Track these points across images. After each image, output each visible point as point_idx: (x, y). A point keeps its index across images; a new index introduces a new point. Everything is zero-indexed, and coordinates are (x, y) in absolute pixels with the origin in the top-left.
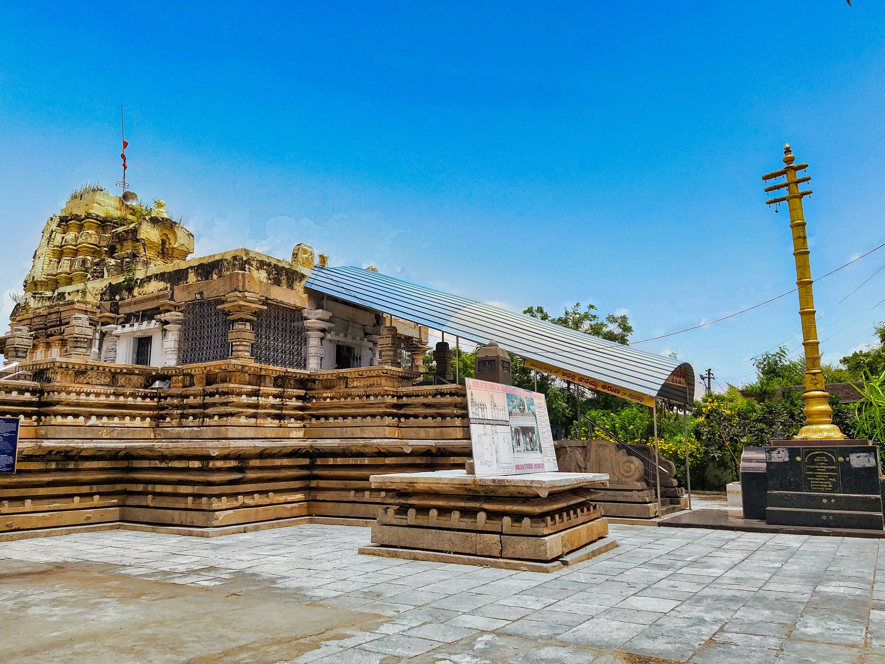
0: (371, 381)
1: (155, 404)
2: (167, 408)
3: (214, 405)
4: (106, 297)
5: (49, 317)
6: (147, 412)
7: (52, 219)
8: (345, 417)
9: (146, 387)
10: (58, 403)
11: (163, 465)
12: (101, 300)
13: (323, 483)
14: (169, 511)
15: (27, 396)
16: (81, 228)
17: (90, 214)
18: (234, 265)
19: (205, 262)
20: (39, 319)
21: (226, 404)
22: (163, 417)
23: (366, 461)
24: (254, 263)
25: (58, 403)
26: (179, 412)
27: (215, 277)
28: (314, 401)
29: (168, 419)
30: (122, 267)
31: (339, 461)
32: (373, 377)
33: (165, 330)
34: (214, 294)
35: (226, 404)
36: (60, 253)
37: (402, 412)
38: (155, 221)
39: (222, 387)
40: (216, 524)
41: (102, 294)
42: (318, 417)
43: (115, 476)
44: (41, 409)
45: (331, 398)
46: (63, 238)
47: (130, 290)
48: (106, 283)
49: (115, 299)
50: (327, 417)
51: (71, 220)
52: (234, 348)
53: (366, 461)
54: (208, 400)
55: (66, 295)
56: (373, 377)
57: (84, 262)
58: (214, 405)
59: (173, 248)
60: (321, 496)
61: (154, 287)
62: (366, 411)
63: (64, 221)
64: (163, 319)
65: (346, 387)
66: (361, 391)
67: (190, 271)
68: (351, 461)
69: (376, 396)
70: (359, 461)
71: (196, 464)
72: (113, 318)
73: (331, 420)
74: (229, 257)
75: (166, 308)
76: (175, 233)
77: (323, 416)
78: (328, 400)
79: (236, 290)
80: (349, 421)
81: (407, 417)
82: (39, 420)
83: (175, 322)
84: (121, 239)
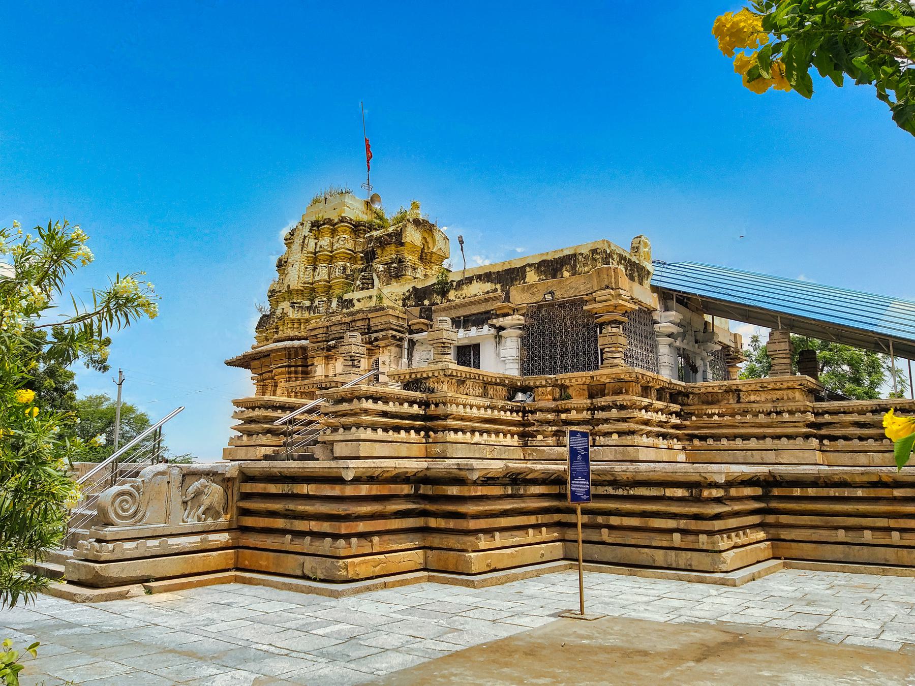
0: (778, 394)
1: (520, 419)
2: (534, 424)
3: (607, 421)
4: (411, 302)
5: (353, 324)
6: (515, 429)
7: (302, 224)
8: (746, 437)
9: (510, 399)
10: (446, 417)
11: (620, 492)
12: (404, 306)
13: (784, 519)
14: (646, 550)
15: (415, 409)
16: (333, 232)
17: (345, 218)
18: (595, 260)
19: (549, 258)
20: (339, 327)
21: (624, 420)
22: (533, 435)
23: (860, 493)
24: (615, 256)
25: (446, 417)
26: (554, 428)
28: (694, 418)
29: (540, 437)
30: (390, 273)
31: (811, 492)
32: (781, 389)
33: (500, 337)
34: (571, 293)
35: (624, 420)
36: (314, 260)
37: (823, 432)
38: (417, 223)
39: (619, 399)
40: (725, 569)
41: (404, 300)
42: (703, 438)
43: (515, 506)
44: (428, 424)
45: (719, 415)
46: (316, 244)
47: (444, 293)
48: (409, 287)
49: (422, 304)
50: (717, 438)
51: (324, 224)
52: (605, 356)
53: (860, 493)
54: (599, 415)
55: (355, 302)
56: (781, 389)
57: (344, 268)
58: (607, 421)
59: (432, 253)
60: (785, 534)
61: (477, 289)
62: (778, 431)
63: (316, 226)
64: (497, 325)
65: (738, 402)
66: (769, 407)
67: (528, 269)
68: (832, 492)
69: (791, 413)
70: (846, 492)
71: (679, 492)
72: (427, 325)
73: (724, 441)
74: (585, 251)
75: (505, 311)
76: (433, 237)
77: (711, 437)
78: (716, 417)
79: (608, 287)
80: (753, 443)
81: (833, 438)
82: (427, 436)
83: (513, 327)
84: (383, 243)
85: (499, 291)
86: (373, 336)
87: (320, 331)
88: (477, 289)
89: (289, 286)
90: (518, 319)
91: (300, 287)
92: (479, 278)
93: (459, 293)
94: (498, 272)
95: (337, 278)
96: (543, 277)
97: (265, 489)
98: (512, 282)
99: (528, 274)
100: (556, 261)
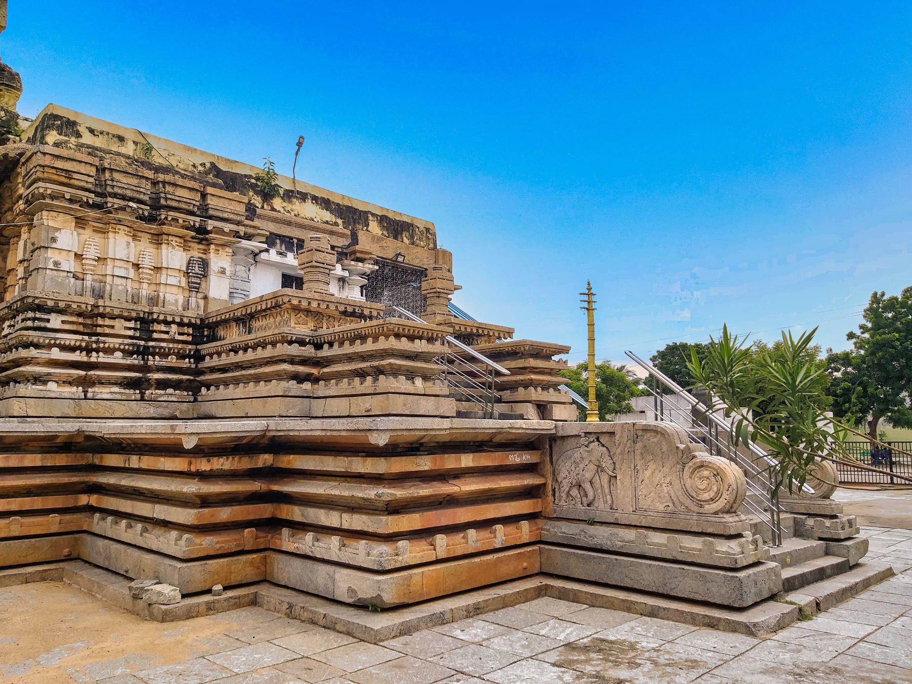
5: (169, 188)
19: (391, 216)
20: (135, 181)
27: (405, 240)
61: (310, 211)
67: (370, 218)
85: (341, 227)
86: (211, 224)
87: (83, 168)
88: (310, 211)
90: (368, 267)
92: (315, 199)
93: (289, 207)
94: (338, 205)
96: (385, 233)
98: (355, 224)
99: (371, 223)
100: (398, 222)
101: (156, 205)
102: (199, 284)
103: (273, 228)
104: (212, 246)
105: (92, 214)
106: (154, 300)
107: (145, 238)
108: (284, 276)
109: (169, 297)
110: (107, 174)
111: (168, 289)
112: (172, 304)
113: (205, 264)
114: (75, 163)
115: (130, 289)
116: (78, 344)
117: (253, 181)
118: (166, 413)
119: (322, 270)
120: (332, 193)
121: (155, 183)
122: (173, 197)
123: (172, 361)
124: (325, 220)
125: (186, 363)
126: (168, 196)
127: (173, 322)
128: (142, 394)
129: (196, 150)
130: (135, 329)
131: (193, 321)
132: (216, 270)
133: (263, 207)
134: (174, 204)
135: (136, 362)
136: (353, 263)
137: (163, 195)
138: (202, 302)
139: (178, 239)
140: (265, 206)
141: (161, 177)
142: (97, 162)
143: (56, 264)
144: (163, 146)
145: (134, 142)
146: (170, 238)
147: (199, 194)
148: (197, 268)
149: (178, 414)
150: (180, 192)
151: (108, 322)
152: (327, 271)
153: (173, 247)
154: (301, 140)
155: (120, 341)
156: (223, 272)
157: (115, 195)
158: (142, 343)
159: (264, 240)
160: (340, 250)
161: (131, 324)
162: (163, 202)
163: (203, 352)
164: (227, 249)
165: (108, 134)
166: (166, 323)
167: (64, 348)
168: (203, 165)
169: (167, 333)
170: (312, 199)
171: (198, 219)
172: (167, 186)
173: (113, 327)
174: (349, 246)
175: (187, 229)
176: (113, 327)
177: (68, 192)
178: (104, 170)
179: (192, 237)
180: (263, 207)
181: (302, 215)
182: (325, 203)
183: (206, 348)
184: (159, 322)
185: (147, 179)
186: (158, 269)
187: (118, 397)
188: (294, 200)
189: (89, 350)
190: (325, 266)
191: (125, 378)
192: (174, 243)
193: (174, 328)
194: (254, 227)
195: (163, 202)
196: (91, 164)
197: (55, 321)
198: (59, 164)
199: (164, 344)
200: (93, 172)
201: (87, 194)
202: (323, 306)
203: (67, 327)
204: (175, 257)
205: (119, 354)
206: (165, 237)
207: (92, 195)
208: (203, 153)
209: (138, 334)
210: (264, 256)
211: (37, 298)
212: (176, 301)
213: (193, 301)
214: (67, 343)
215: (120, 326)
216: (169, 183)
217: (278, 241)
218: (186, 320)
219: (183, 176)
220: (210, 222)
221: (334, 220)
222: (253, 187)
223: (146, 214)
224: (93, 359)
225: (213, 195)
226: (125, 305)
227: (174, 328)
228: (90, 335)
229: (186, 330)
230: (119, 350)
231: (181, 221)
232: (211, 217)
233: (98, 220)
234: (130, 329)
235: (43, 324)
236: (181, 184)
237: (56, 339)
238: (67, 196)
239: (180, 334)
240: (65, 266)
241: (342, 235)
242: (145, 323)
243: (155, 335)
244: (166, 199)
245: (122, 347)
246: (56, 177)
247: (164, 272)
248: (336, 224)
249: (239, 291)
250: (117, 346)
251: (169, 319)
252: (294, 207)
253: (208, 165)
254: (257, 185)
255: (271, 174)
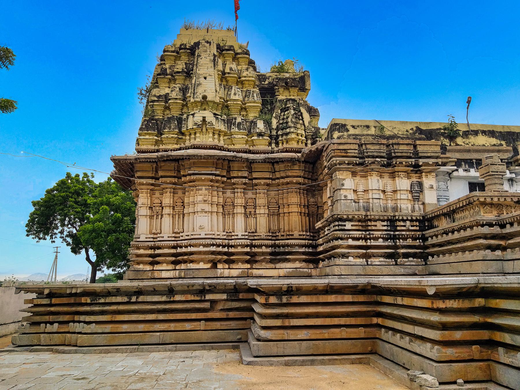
5: (395, 147)
20: (377, 147)
85: (505, 146)
86: (421, 161)
87: (352, 146)
88: (482, 140)
89: (204, 97)
91: (217, 100)
92: (484, 132)
93: (467, 141)
94: (500, 132)
95: (254, 102)
97: (433, 303)
101: (390, 157)
102: (419, 196)
103: (458, 156)
104: (424, 174)
105: (359, 168)
106: (395, 209)
107: (386, 176)
108: (470, 184)
109: (403, 206)
110: (364, 147)
111: (402, 201)
112: (405, 210)
113: (420, 185)
114: (348, 145)
115: (382, 204)
116: (360, 236)
117: (442, 131)
118: (410, 271)
119: (497, 176)
120: (495, 126)
121: (388, 146)
122: (398, 151)
123: (410, 242)
124: (492, 144)
125: (417, 243)
126: (396, 151)
127: (407, 220)
128: (396, 261)
129: (407, 122)
130: (387, 226)
131: (418, 218)
132: (428, 187)
133: (450, 145)
134: (399, 154)
135: (390, 244)
136: (517, 167)
137: (393, 151)
138: (421, 207)
139: (403, 173)
140: (452, 144)
141: (391, 141)
142: (358, 142)
143: (345, 196)
144: (389, 125)
145: (374, 127)
146: (400, 173)
147: (412, 146)
148: (416, 188)
149: (417, 272)
150: (402, 147)
151: (373, 223)
152: (501, 176)
153: (402, 178)
154: (470, 99)
155: (380, 233)
156: (432, 187)
157: (368, 157)
158: (392, 233)
159: (454, 164)
160: (506, 161)
161: (385, 223)
162: (393, 155)
163: (427, 236)
164: (433, 174)
165: (361, 126)
166: (404, 221)
167: (354, 239)
168: (412, 129)
169: (405, 226)
170: (482, 133)
171: (413, 160)
172: (394, 146)
173: (376, 226)
174: (512, 157)
175: (408, 166)
176: (376, 226)
177: (347, 160)
178: (362, 145)
179: (411, 171)
180: (450, 145)
181: (477, 144)
182: (491, 133)
183: (428, 233)
184: (399, 221)
185: (384, 144)
186: (395, 191)
187: (384, 263)
188: (470, 136)
189: (366, 239)
190: (499, 173)
191: (386, 253)
192: (402, 176)
193: (408, 223)
194: (447, 158)
195: (393, 155)
196: (356, 144)
197: (348, 225)
198: (341, 147)
199: (404, 233)
200: (356, 147)
201: (355, 159)
202: (502, 200)
203: (354, 228)
204: (403, 183)
205: (381, 240)
206: (397, 173)
207: (358, 159)
208: (411, 123)
209: (389, 228)
210: (455, 174)
211: (339, 215)
212: (407, 208)
213: (416, 206)
214: (355, 236)
215: (379, 225)
216: (395, 144)
217: (463, 163)
218: (414, 218)
219: (402, 138)
220: (420, 160)
221: (499, 142)
222: (443, 134)
223: (385, 163)
224: (369, 244)
225: (420, 145)
226: (380, 213)
227: (408, 223)
228: (365, 231)
229: (415, 223)
230: (381, 238)
231: (404, 163)
232: (421, 158)
233: (362, 171)
234: (385, 226)
235: (343, 228)
236: (402, 143)
237: (350, 234)
238: (346, 162)
239: (412, 226)
240: (349, 197)
241: (507, 151)
242: (392, 222)
243: (398, 228)
244: (395, 153)
245: (382, 236)
246: (340, 154)
247: (398, 192)
248: (501, 145)
249: (443, 197)
250: (379, 236)
251: (405, 218)
252: (470, 140)
253: (415, 129)
254: (445, 133)
255: (453, 124)
